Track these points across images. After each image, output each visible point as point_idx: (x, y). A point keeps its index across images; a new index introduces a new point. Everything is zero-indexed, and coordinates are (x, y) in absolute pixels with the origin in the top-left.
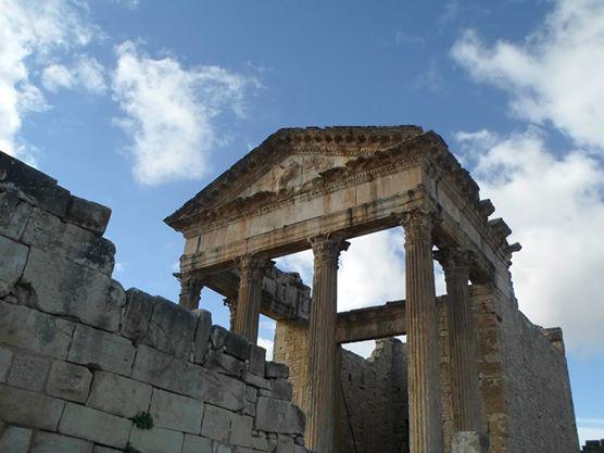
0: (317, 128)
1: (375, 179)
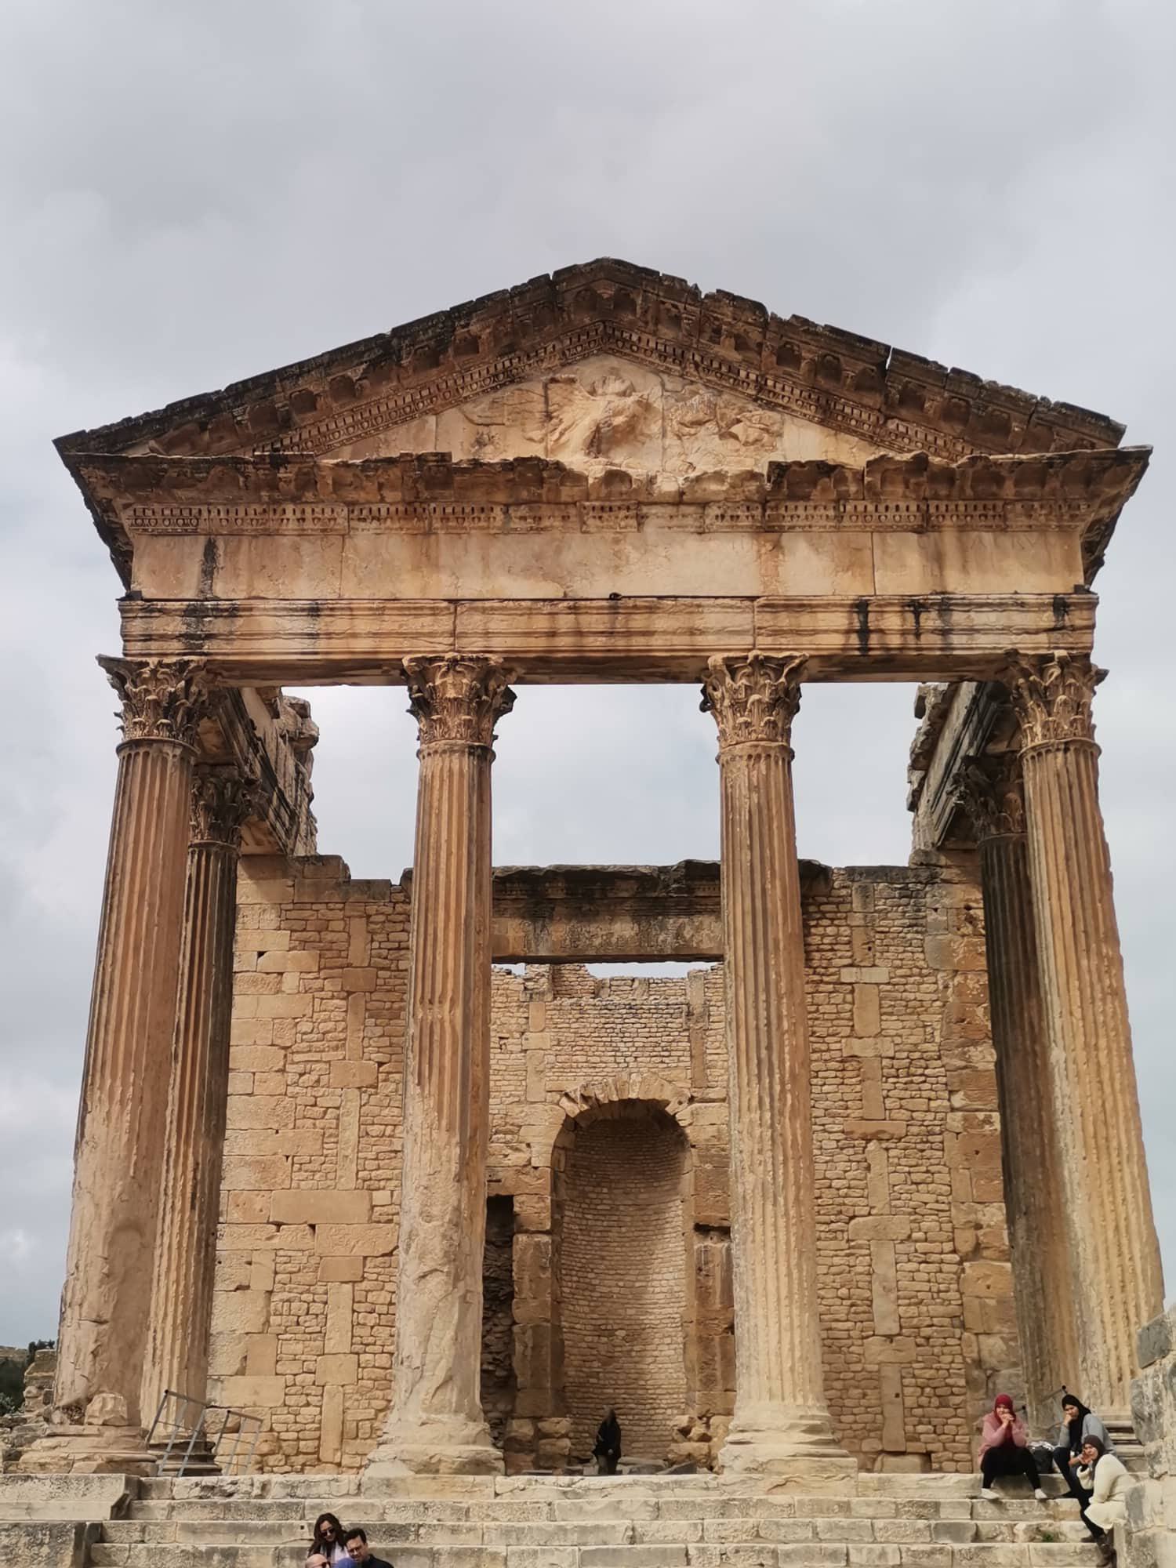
0: (759, 307)
1: (937, 528)
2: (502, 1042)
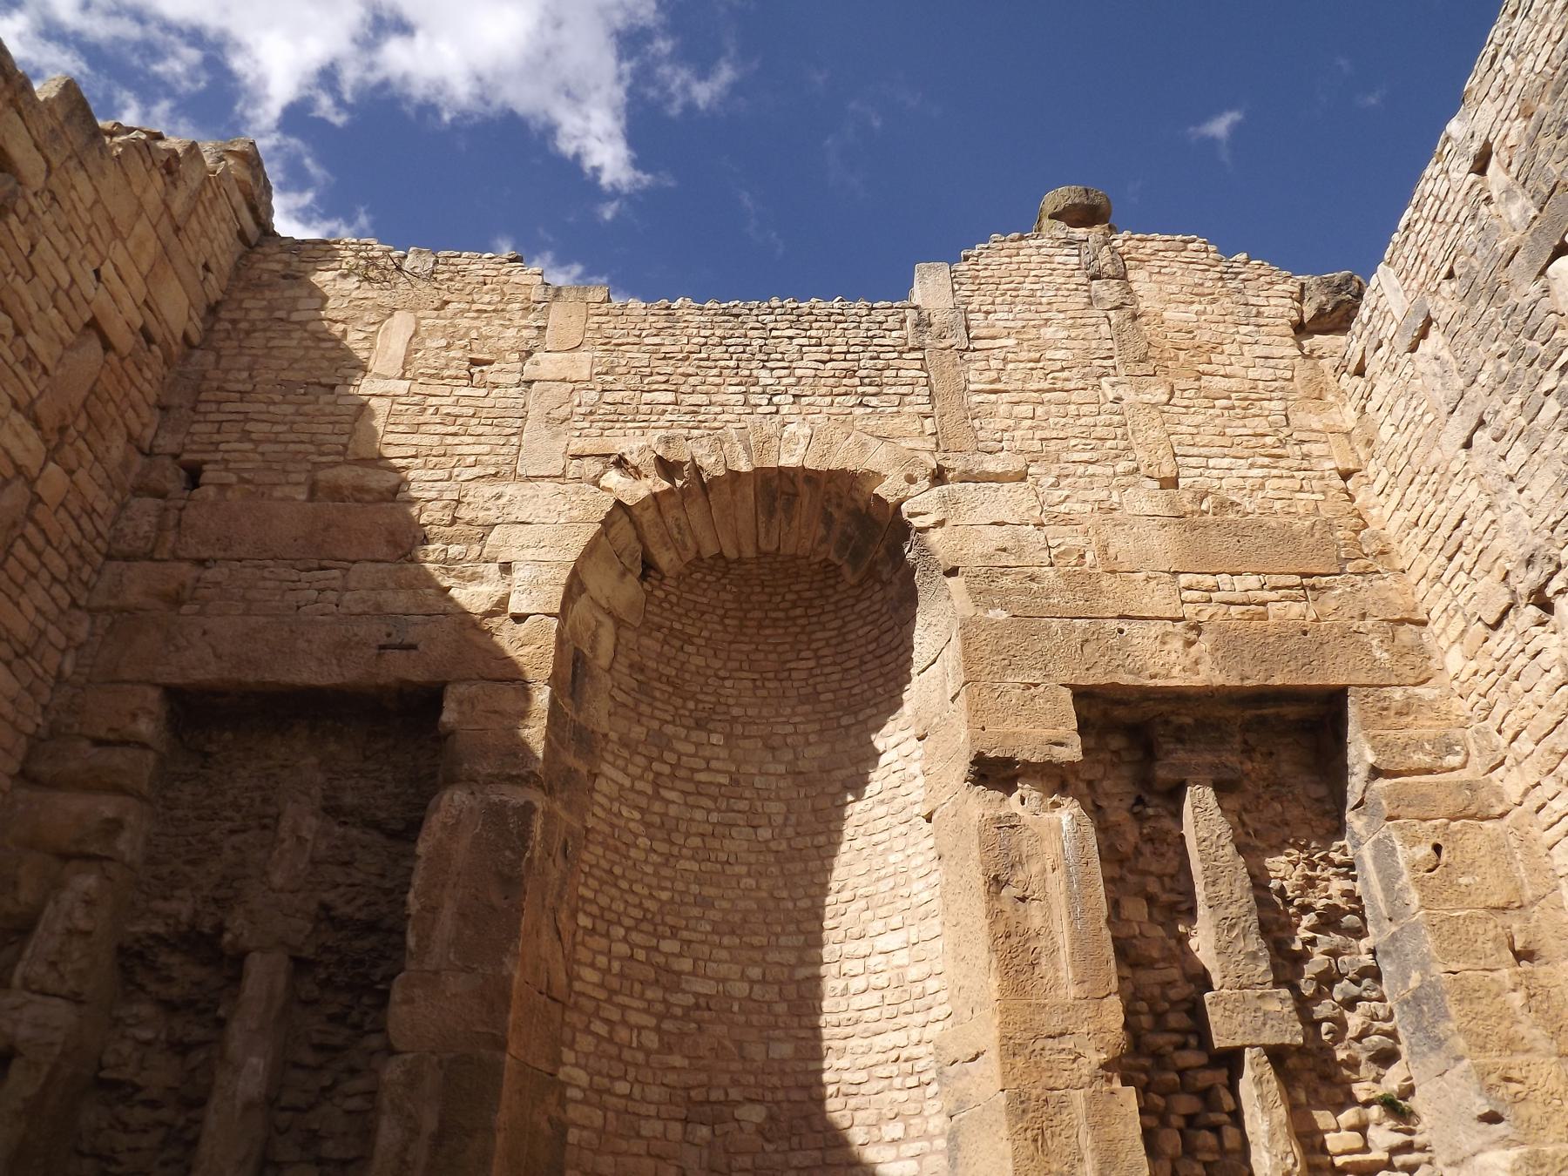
2: (475, 370)
